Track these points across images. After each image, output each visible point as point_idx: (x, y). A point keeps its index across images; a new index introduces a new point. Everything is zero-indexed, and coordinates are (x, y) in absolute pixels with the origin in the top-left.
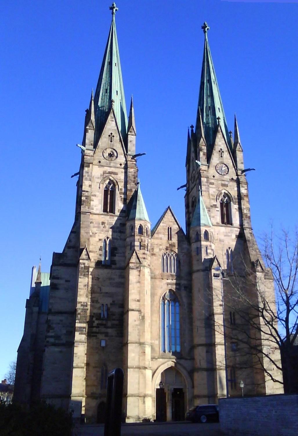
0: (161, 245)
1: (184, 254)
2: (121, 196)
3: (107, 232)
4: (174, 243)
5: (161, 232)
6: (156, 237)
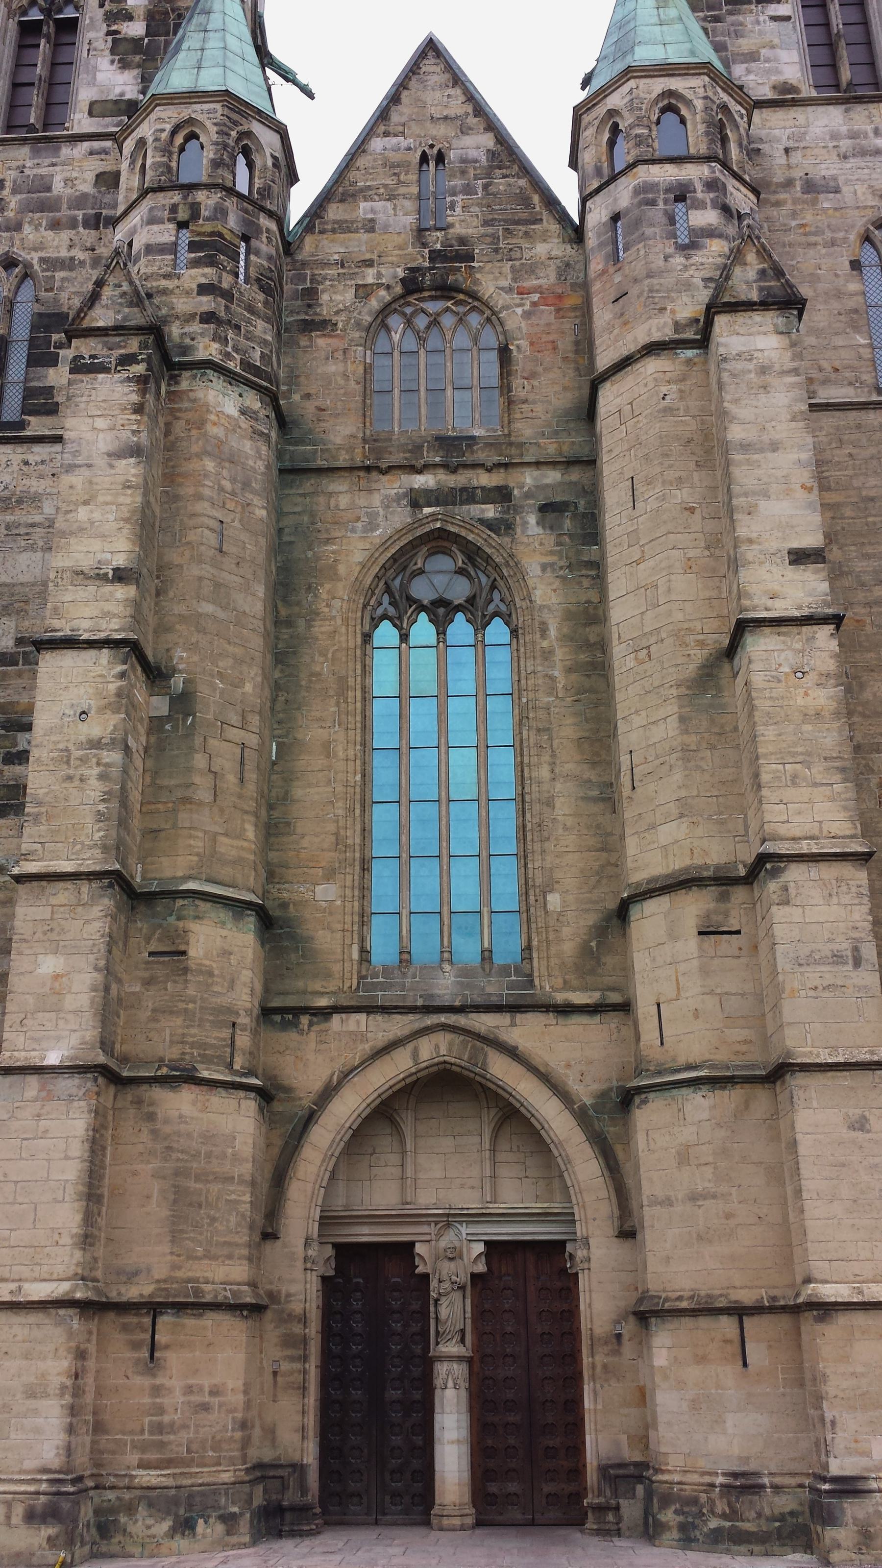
0: (369, 263)
1: (535, 297)
2: (114, 28)
3: (8, 229)
4: (462, 241)
5: (369, 188)
6: (335, 222)
